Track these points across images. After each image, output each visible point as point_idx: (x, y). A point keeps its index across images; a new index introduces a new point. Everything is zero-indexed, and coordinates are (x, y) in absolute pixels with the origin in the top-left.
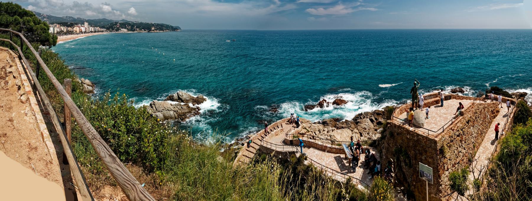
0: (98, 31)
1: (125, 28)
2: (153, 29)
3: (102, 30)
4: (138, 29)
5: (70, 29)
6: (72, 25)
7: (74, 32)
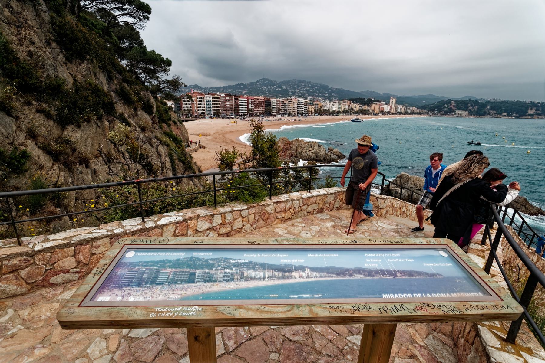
0: (412, 113)
1: (466, 109)
2: (530, 112)
3: (419, 110)
4: (492, 112)
5: (366, 107)
6: (369, 102)
7: (371, 111)
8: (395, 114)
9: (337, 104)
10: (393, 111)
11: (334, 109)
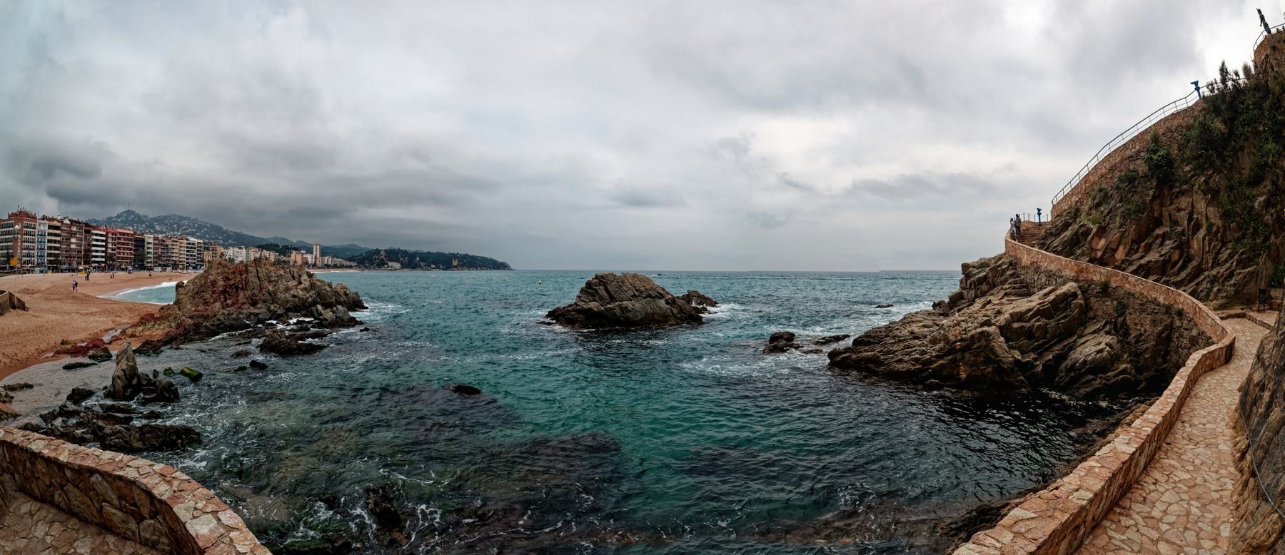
0: (342, 267)
9: (244, 251)
10: (319, 263)
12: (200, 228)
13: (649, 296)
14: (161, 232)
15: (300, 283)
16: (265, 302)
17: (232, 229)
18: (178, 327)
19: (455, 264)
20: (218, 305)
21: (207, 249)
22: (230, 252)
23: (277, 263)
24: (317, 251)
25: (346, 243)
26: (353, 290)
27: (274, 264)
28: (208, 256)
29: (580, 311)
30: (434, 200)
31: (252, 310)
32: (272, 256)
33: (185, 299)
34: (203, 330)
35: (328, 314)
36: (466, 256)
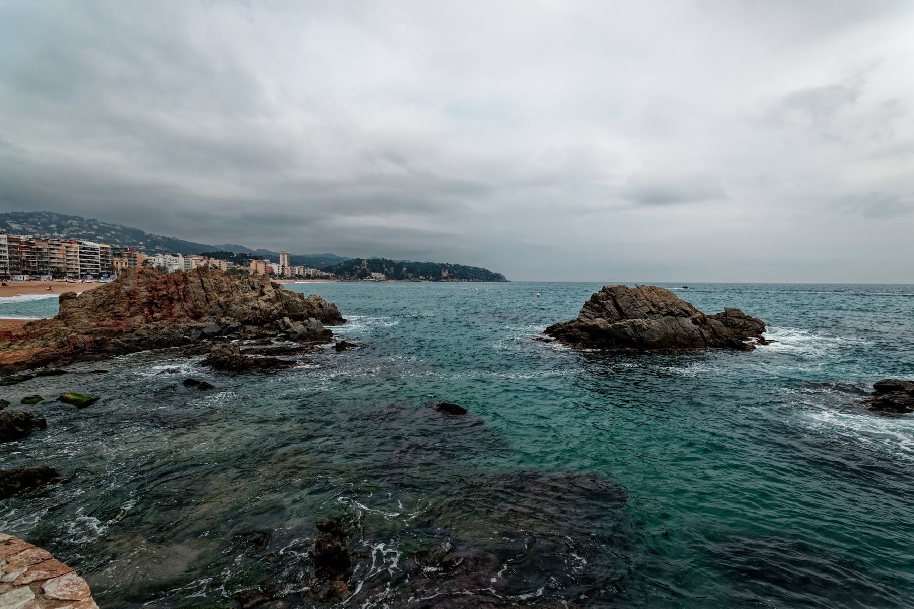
0: (316, 277)
3: (324, 274)
5: (238, 267)
8: (291, 278)
9: (181, 259)
10: (288, 273)
11: (176, 268)
12: (102, 230)
13: (671, 313)
14: (24, 232)
15: (263, 294)
16: (213, 314)
17: (159, 234)
18: (62, 345)
19: (445, 274)
20: (139, 318)
21: (120, 255)
22: (159, 260)
23: (231, 272)
24: (284, 261)
25: (321, 253)
26: (329, 302)
27: (226, 274)
28: (120, 264)
29: (583, 328)
30: (419, 207)
31: (194, 323)
32: (224, 266)
33: (76, 313)
34: (110, 348)
35: (298, 327)
36: (457, 267)
